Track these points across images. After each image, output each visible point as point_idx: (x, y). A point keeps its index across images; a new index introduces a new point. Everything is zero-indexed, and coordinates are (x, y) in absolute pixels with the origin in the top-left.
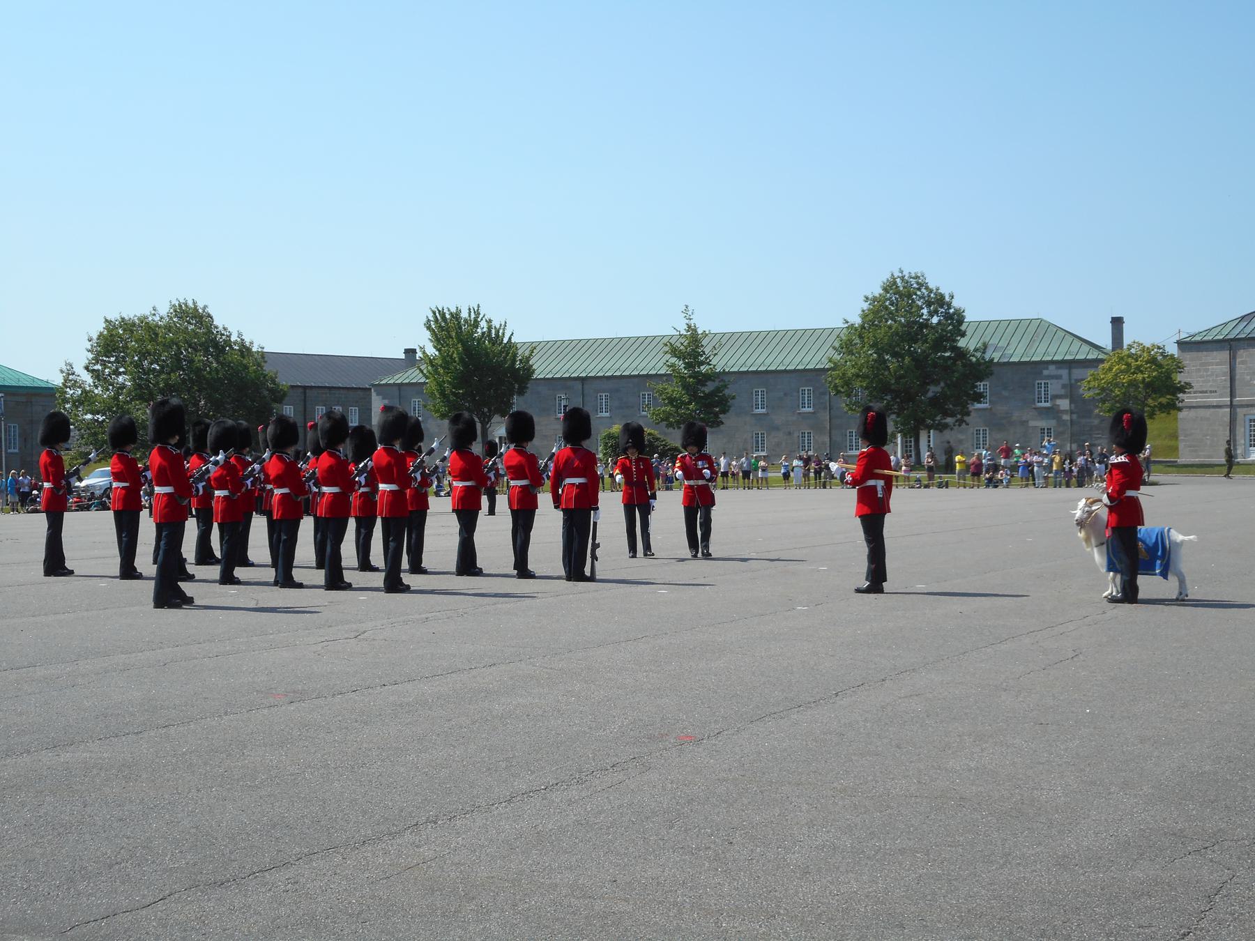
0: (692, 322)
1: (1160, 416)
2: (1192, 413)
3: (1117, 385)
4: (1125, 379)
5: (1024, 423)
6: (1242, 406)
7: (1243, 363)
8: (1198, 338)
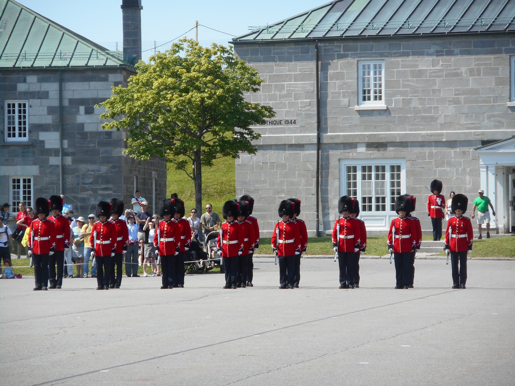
1: (220, 161)
2: (271, 156)
3: (158, 110)
4: (174, 100)
6: (336, 146)
7: (339, 76)
8: (266, 36)
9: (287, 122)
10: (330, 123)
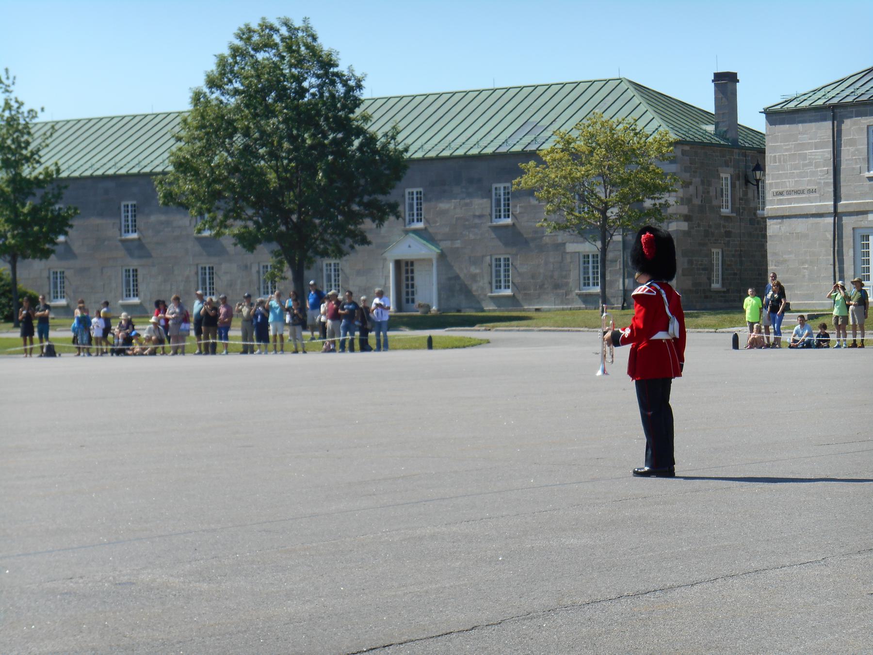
0: (13, 96)
5: (560, 247)
7: (852, 142)
8: (792, 105)
9: (810, 191)
10: (843, 190)
